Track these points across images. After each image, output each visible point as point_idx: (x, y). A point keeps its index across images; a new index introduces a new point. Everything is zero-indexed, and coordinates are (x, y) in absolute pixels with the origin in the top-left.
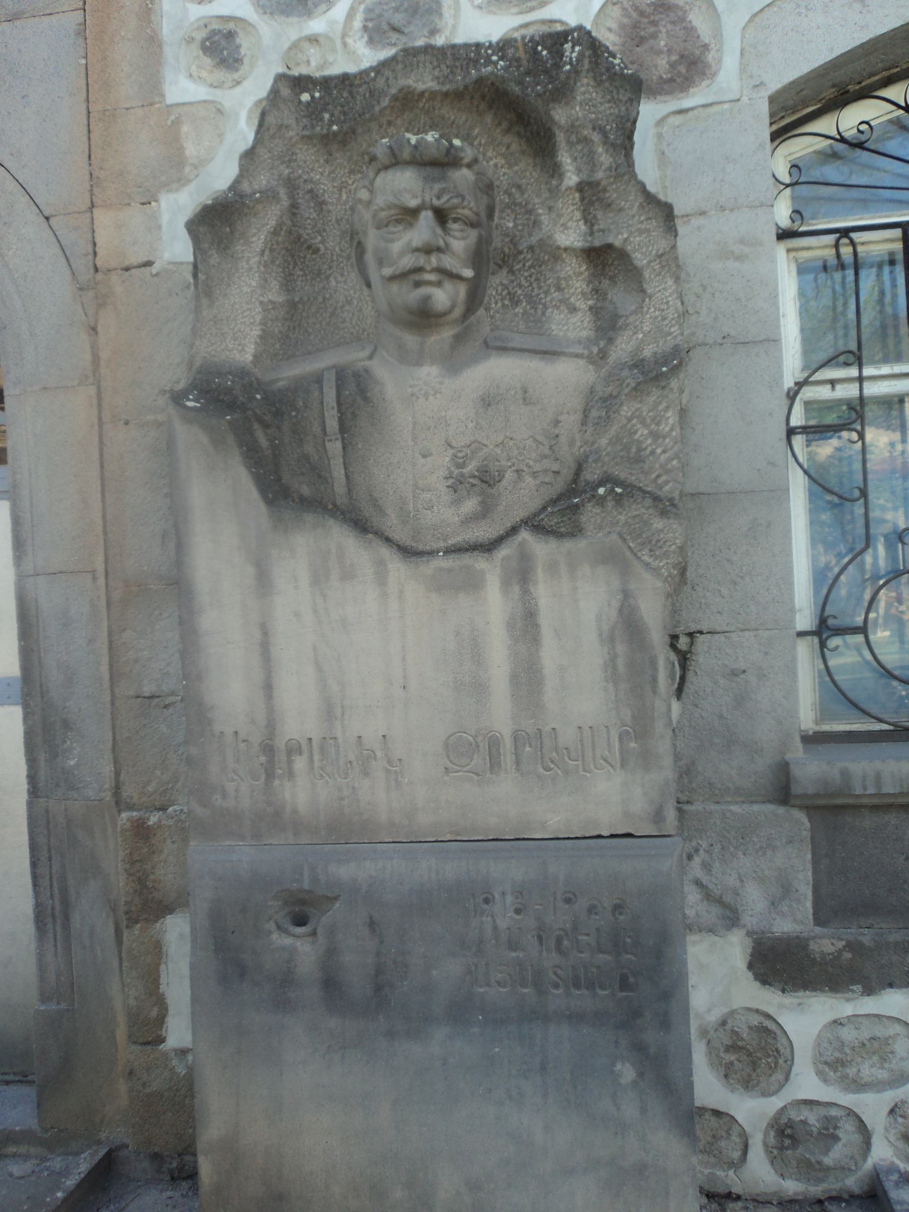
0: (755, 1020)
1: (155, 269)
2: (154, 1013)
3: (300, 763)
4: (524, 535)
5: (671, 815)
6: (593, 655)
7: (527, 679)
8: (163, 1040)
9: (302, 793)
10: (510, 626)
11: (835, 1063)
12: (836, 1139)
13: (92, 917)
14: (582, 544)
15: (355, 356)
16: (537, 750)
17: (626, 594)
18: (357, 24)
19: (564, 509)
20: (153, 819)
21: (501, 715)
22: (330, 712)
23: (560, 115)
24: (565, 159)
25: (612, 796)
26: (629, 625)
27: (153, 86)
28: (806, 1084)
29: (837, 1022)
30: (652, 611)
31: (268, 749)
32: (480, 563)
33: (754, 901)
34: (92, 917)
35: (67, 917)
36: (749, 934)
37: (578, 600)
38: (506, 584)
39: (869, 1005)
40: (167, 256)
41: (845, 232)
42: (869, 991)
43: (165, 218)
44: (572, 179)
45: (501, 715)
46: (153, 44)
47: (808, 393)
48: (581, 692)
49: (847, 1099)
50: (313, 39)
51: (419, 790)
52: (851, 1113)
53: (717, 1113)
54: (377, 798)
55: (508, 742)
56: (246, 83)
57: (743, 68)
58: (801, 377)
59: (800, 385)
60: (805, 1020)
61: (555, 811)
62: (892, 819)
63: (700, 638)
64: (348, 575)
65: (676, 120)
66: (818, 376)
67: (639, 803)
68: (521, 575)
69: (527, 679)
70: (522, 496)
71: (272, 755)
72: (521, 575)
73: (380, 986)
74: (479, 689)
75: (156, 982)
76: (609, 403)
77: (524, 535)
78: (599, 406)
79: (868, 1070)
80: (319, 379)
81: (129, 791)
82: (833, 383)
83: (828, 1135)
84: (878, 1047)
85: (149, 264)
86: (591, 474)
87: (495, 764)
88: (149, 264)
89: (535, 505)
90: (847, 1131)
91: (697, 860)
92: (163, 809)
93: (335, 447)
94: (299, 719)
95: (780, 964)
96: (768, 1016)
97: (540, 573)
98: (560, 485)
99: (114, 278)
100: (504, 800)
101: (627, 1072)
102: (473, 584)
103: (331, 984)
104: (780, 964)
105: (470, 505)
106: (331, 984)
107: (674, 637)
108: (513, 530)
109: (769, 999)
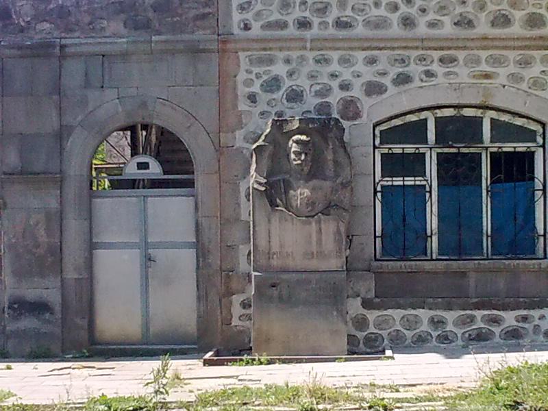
0: (362, 316)
1: (234, 148)
2: (229, 317)
3: (275, 256)
4: (320, 214)
5: (345, 267)
6: (332, 237)
7: (319, 241)
8: (231, 324)
9: (275, 262)
10: (317, 232)
11: (377, 326)
12: (377, 341)
13: (214, 297)
14: (331, 217)
15: (287, 176)
16: (321, 255)
17: (338, 226)
18: (285, 97)
19: (326, 211)
20: (231, 273)
21: (314, 249)
22: (281, 246)
23: (329, 135)
24: (330, 144)
25: (335, 263)
26: (338, 232)
27: (235, 106)
28: (372, 329)
29: (379, 316)
30: (343, 229)
31: (269, 253)
32: (310, 219)
33: (363, 294)
34: (214, 297)
35: (207, 297)
36: (362, 298)
37: (329, 227)
38: (316, 223)
39: (385, 312)
40: (238, 145)
41: (390, 149)
42: (386, 310)
43: (237, 137)
44: (331, 147)
45: (314, 249)
46: (236, 96)
47: (382, 183)
48: (329, 244)
49: (380, 332)
50: (274, 99)
51: (298, 262)
52: (380, 334)
53: (354, 336)
54: (291, 263)
55: (315, 253)
56: (258, 107)
57: (368, 116)
58: (380, 179)
59: (380, 181)
60: (372, 316)
61: (324, 266)
62: (391, 275)
63: (354, 237)
64: (286, 221)
65: (353, 126)
66: (384, 179)
67: (340, 265)
68: (319, 222)
69: (319, 241)
70: (320, 207)
71: (269, 255)
72: (319, 222)
73: (290, 297)
74: (310, 243)
75: (230, 310)
76: (337, 191)
77: (320, 214)
78: (334, 191)
79: (384, 326)
80: (279, 180)
81: (224, 268)
82: (387, 181)
83: (376, 340)
84: (386, 321)
85: (233, 146)
86: (333, 204)
87: (313, 257)
88: (233, 146)
89: (322, 209)
90: (380, 338)
91: (351, 283)
92: (232, 271)
93: (284, 196)
94: (275, 248)
95: (367, 304)
96: (364, 315)
97: (322, 222)
98: (327, 205)
99: (224, 149)
100: (314, 264)
101: (335, 313)
102: (310, 223)
103: (280, 298)
104: (367, 304)
105: (310, 208)
106: (280, 298)
107: (348, 236)
108: (317, 214)
109: (365, 312)
